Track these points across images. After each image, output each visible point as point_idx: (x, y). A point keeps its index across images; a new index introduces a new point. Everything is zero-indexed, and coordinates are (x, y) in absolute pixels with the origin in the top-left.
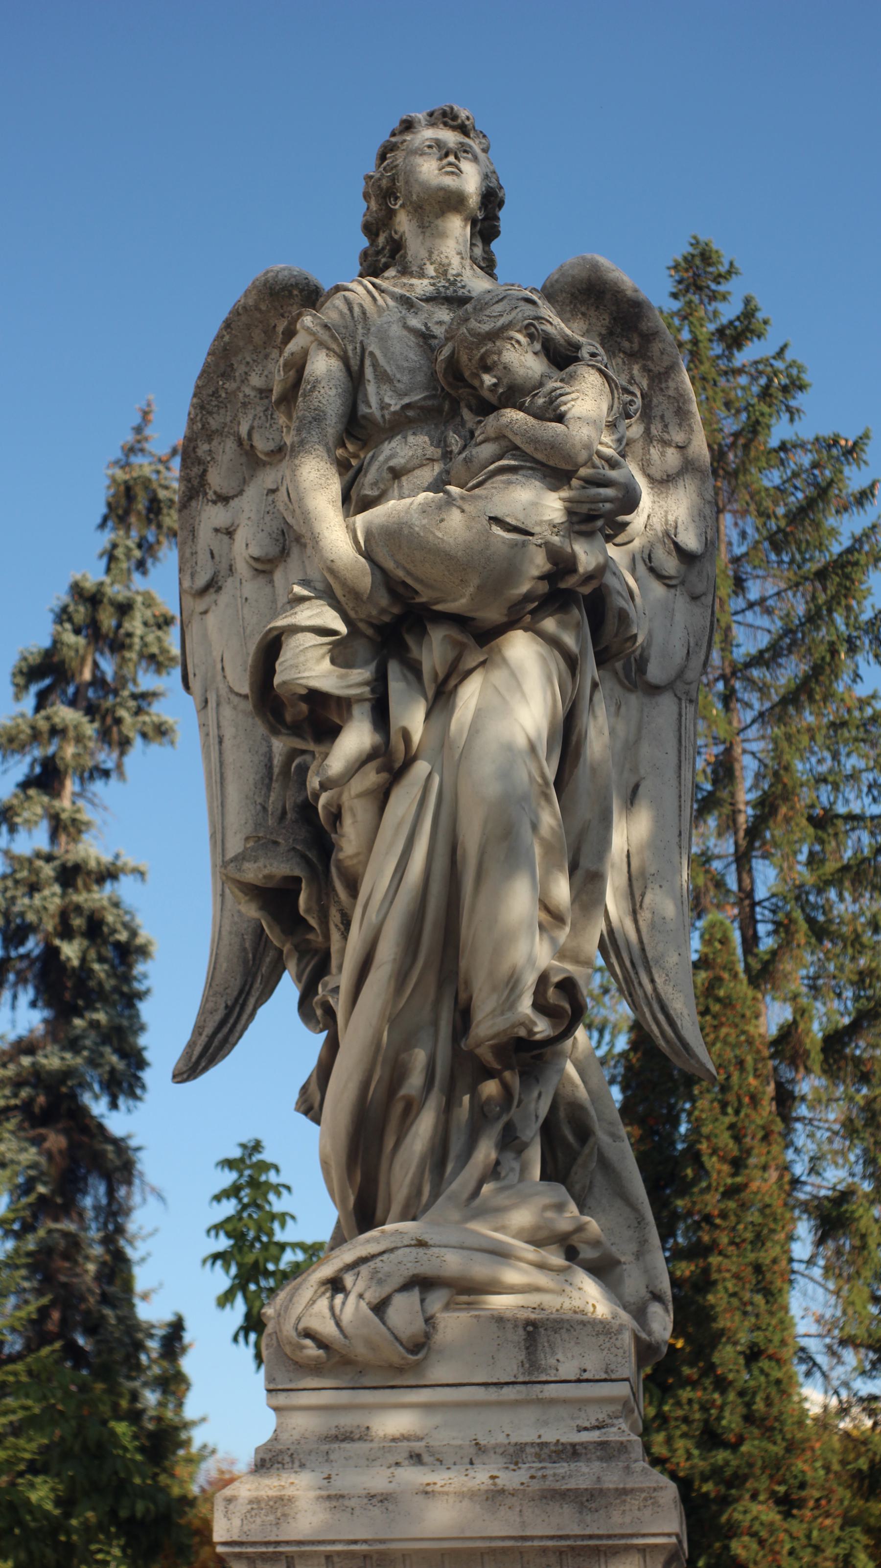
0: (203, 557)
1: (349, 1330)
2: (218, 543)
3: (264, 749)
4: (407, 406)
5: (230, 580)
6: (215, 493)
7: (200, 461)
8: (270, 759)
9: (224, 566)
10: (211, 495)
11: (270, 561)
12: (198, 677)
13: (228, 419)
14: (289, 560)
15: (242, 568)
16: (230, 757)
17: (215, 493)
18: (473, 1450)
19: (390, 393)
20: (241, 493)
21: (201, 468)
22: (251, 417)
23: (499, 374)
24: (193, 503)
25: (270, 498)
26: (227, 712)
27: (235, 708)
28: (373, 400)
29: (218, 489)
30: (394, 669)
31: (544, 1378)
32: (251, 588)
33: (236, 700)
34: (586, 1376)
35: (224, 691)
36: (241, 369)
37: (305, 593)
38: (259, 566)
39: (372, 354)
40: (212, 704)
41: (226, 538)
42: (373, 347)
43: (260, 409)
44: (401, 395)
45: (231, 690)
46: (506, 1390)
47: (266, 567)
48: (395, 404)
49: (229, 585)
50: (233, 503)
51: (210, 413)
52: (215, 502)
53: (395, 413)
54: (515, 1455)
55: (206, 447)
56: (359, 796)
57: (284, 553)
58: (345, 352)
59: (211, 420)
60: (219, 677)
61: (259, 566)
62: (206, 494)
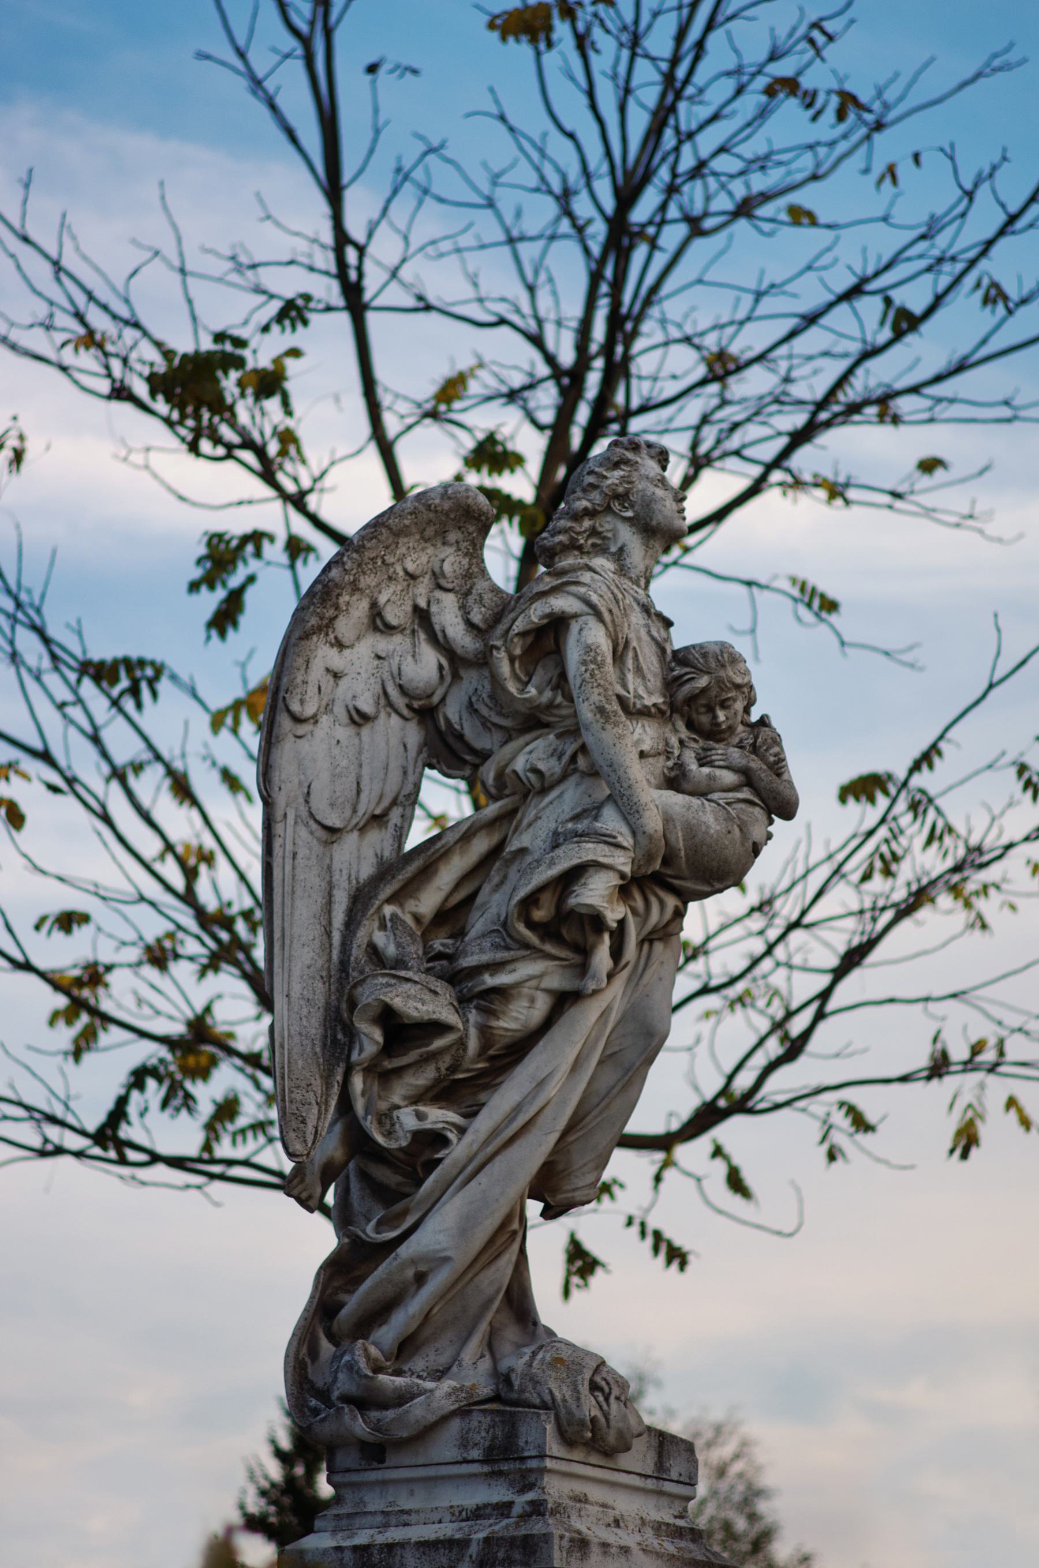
0: (312, 690)
1: (612, 1423)
2: (328, 682)
3: (328, 878)
4: (654, 705)
5: (325, 716)
6: (336, 638)
7: (337, 607)
8: (331, 886)
9: (324, 703)
10: (332, 636)
12: (283, 792)
13: (374, 584)
14: (376, 722)
15: (339, 711)
17: (336, 638)
18: (639, 1522)
20: (352, 646)
21: (336, 613)
22: (391, 591)
23: (729, 715)
24: (315, 638)
25: (376, 662)
26: (303, 832)
27: (312, 833)
28: (631, 687)
29: (340, 636)
31: (665, 1476)
32: (344, 733)
33: (314, 826)
34: (682, 1479)
35: (304, 813)
36: (402, 550)
38: (356, 717)
39: (634, 648)
41: (332, 680)
42: (634, 644)
43: (400, 588)
44: (650, 693)
45: (311, 815)
46: (649, 1481)
48: (649, 701)
49: (325, 720)
50: (347, 652)
51: (364, 573)
52: (332, 645)
53: (646, 707)
54: (659, 1528)
55: (347, 598)
56: (548, 991)
58: (617, 639)
59: (362, 578)
60: (301, 800)
61: (356, 717)
62: (327, 635)
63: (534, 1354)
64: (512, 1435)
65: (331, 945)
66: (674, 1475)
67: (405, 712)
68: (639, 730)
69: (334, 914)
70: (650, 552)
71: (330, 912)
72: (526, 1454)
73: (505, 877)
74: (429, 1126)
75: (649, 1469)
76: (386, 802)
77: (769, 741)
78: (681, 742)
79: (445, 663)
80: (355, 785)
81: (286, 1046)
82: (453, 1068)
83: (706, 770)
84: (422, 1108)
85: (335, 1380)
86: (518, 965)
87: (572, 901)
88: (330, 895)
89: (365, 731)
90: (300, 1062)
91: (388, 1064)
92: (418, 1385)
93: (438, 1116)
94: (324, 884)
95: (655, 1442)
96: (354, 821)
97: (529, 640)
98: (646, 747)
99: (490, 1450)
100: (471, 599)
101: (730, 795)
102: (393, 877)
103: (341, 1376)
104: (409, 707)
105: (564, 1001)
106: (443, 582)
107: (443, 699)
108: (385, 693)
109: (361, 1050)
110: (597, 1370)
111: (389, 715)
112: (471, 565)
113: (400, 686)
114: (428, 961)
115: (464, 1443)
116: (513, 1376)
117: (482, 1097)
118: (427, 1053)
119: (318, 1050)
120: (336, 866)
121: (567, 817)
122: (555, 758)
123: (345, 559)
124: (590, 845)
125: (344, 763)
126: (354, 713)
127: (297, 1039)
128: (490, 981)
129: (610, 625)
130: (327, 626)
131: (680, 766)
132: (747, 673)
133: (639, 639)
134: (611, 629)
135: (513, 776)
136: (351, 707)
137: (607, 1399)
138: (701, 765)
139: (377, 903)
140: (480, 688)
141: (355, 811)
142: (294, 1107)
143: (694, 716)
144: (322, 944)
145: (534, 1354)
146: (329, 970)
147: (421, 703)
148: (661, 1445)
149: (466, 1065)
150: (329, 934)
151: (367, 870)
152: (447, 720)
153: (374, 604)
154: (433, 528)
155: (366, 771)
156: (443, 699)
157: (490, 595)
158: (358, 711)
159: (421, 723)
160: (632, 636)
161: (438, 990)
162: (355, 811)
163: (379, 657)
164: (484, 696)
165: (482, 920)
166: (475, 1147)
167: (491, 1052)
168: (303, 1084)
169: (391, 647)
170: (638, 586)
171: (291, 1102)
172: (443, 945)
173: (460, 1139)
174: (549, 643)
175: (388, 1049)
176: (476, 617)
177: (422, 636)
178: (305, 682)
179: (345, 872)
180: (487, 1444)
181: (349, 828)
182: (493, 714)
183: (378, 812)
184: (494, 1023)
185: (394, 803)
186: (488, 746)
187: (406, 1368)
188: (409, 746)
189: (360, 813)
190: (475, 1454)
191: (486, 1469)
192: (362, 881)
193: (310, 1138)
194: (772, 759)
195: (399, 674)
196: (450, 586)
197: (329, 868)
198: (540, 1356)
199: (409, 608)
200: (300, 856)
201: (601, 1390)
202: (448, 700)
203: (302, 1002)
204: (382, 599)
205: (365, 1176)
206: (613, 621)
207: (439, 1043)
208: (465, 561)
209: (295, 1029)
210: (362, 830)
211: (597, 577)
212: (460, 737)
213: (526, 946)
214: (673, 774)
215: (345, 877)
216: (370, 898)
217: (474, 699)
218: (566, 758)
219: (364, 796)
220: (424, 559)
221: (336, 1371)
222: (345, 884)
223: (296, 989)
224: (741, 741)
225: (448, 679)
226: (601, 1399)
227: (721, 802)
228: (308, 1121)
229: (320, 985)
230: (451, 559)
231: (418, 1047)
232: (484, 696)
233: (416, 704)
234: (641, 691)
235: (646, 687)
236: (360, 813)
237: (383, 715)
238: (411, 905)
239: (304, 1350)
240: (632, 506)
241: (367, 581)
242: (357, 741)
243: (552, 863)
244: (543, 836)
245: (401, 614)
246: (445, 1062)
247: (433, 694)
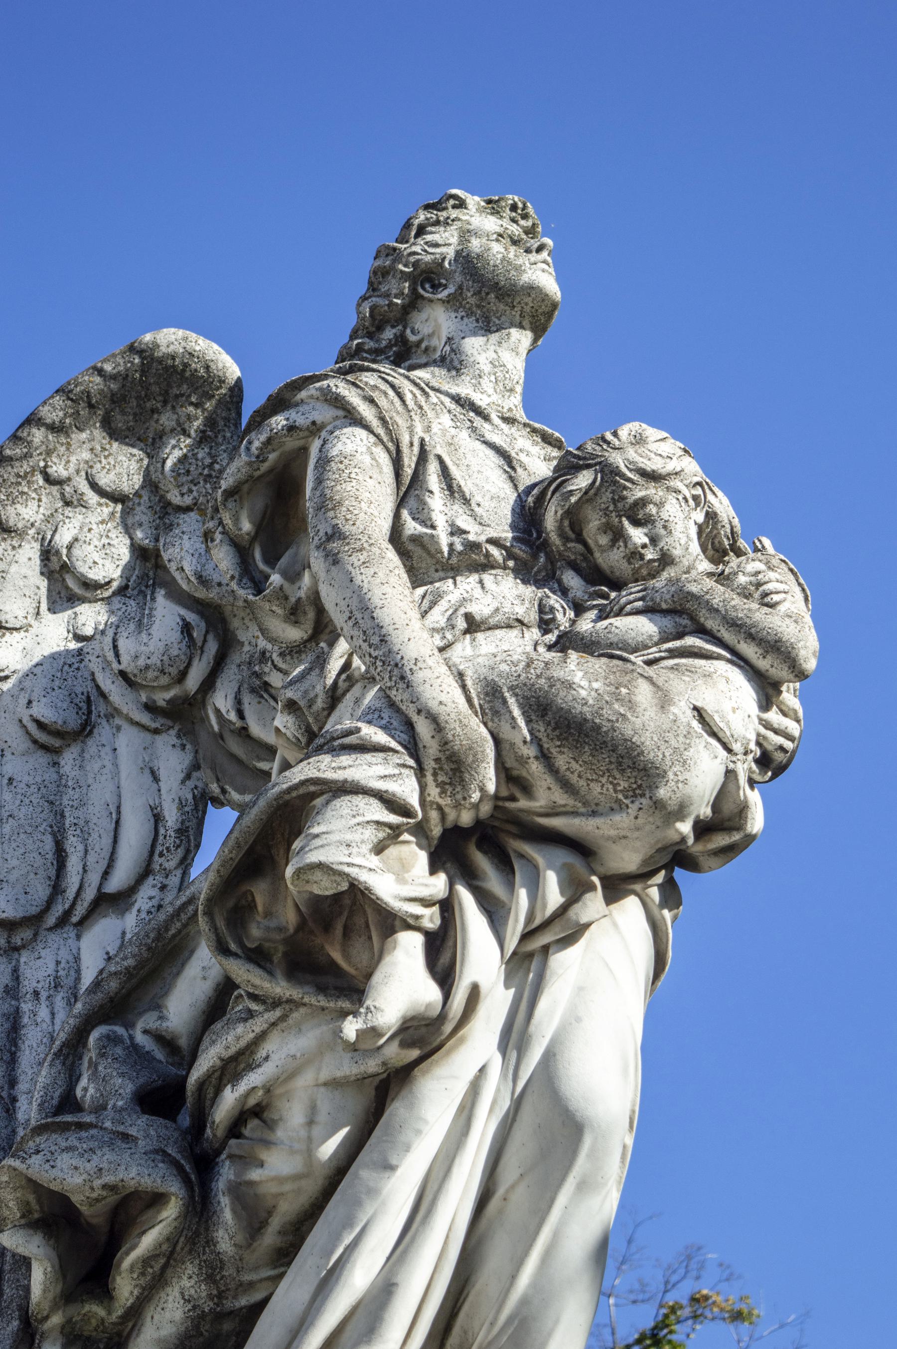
11: (58, 734)
19: (465, 517)
30: (466, 897)
37: (380, 737)
47: (56, 743)
57: (84, 731)
67: (144, 718)
79: (191, 617)
80: (49, 844)
86: (268, 1046)
89: (68, 759)
96: (58, 910)
97: (260, 502)
104: (150, 708)
106: (174, 497)
107: (209, 684)
108: (103, 695)
111: (119, 728)
113: (123, 674)
118: (146, 1261)
126: (32, 728)
129: (375, 423)
134: (381, 431)
136: (26, 721)
141: (57, 889)
147: (169, 695)
152: (218, 711)
153: (47, 553)
158: (40, 725)
161: (133, 1131)
162: (57, 889)
177: (160, 594)
184: (255, 1175)
188: (163, 774)
195: (117, 655)
196: (188, 500)
204: (63, 538)
206: (382, 419)
210: (82, 923)
212: (244, 733)
213: (276, 1003)
219: (74, 864)
233: (162, 698)
234: (464, 522)
235: (474, 516)
236: (71, 893)
237: (103, 731)
238: (148, 1021)
241: (29, 512)
242: (50, 775)
247: (182, 676)
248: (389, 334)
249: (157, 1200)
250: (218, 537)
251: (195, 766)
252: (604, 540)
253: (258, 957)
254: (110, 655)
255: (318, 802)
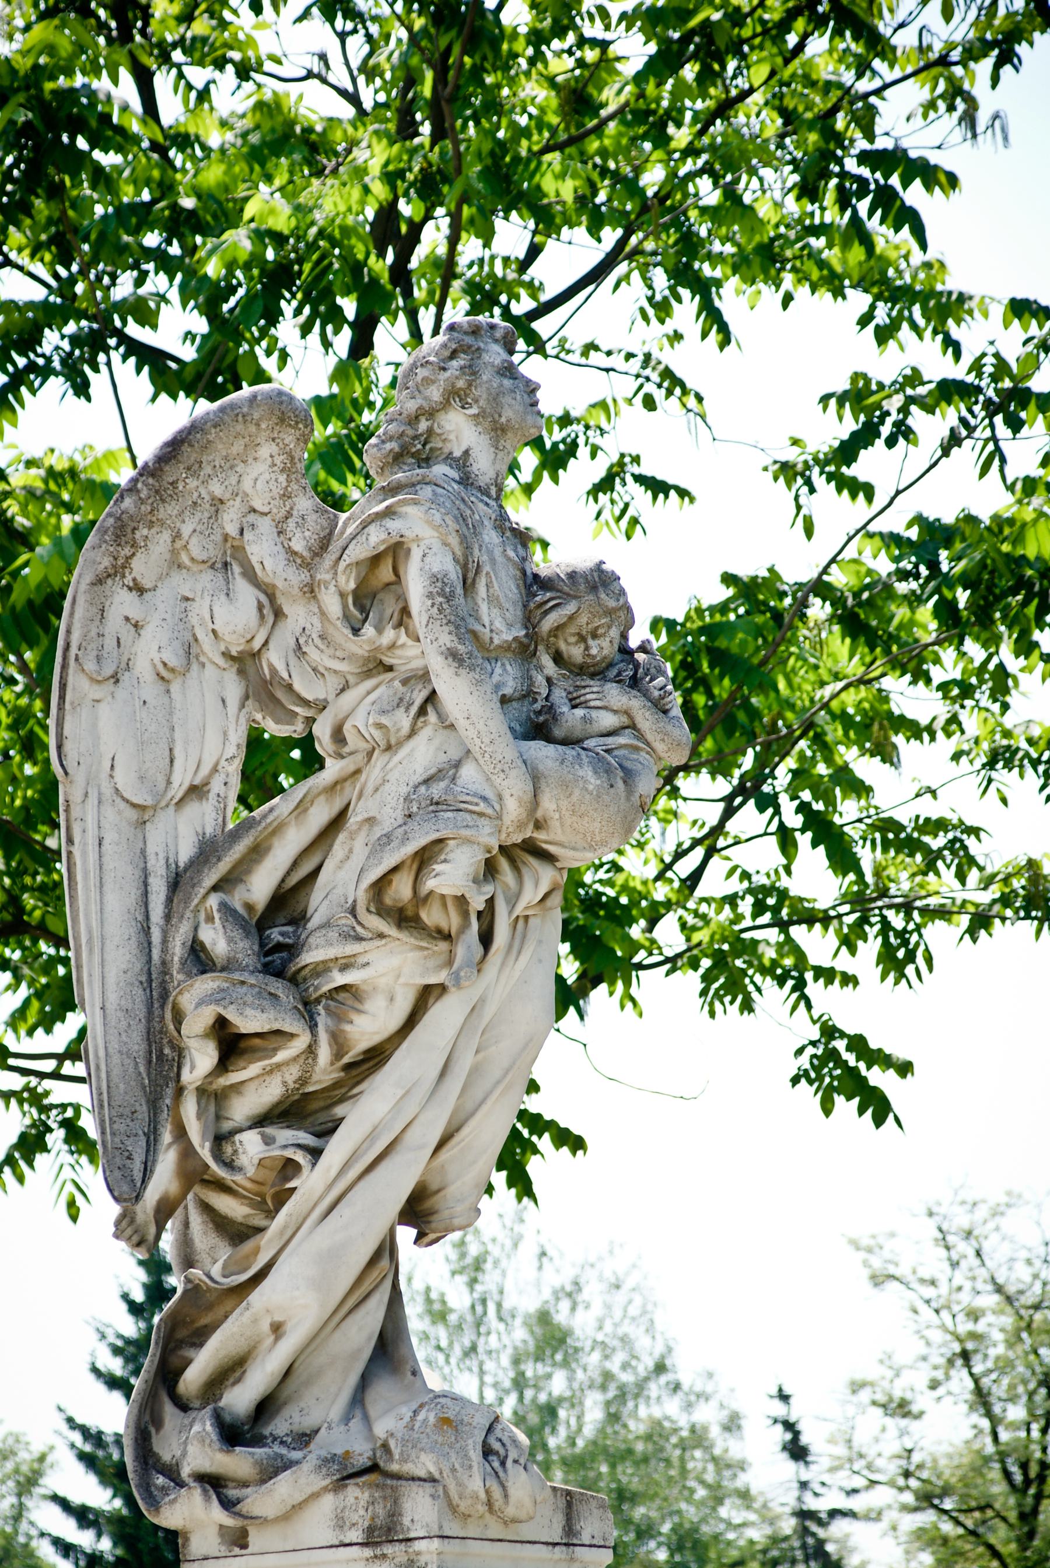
0: (110, 643)
2: (127, 633)
7: (134, 545)
9: (125, 659)
11: (172, 670)
16: (109, 863)
24: (109, 581)
26: (110, 814)
27: (119, 812)
28: (486, 620)
32: (150, 690)
33: (123, 805)
35: (108, 791)
36: (208, 469)
40: (93, 799)
42: (487, 568)
43: (206, 515)
50: (147, 596)
51: (163, 501)
52: (130, 589)
55: (145, 532)
56: (406, 985)
62: (123, 576)
63: (415, 1413)
64: (394, 1515)
65: (150, 943)
66: (586, 1539)
67: (221, 661)
68: (498, 670)
69: (151, 906)
70: (501, 455)
71: (146, 904)
72: (412, 1535)
73: (351, 851)
74: (277, 1153)
75: (556, 1534)
76: (205, 771)
77: (653, 671)
78: (549, 680)
79: (263, 598)
81: (103, 1067)
82: (303, 1081)
83: (579, 712)
84: (269, 1130)
85: (184, 1454)
87: (430, 884)
88: (146, 884)
90: (122, 1086)
91: (224, 1081)
92: (282, 1456)
93: (288, 1138)
94: (138, 873)
95: (562, 1503)
98: (508, 691)
99: (370, 1530)
100: (291, 523)
101: (610, 740)
102: (219, 859)
103: (191, 1449)
105: (426, 996)
109: (193, 1068)
110: (490, 1429)
112: (289, 481)
113: (214, 631)
114: (266, 955)
115: (340, 1523)
116: (392, 1443)
117: (339, 1111)
119: (142, 1069)
120: (151, 849)
121: (420, 779)
122: (402, 709)
123: (140, 485)
124: (450, 814)
125: (152, 728)
127: (116, 1059)
128: (340, 979)
130: (124, 567)
131: (550, 709)
132: (622, 592)
133: (493, 561)
135: (354, 731)
137: (503, 1464)
138: (574, 707)
139: (202, 891)
140: (308, 626)
141: (169, 782)
142: (117, 1140)
143: (563, 646)
144: (140, 944)
145: (415, 1413)
146: (150, 974)
148: (569, 1505)
149: (315, 1077)
150: (146, 931)
151: (185, 852)
154: (242, 442)
155: (178, 735)
156: (266, 643)
157: (315, 516)
158: (165, 664)
159: (241, 672)
160: (485, 558)
163: (187, 599)
164: (315, 636)
165: (326, 902)
166: (334, 1173)
167: (346, 1059)
168: (127, 1111)
169: (199, 587)
170: (489, 496)
171: (113, 1134)
172: (282, 934)
173: (314, 1165)
174: (385, 573)
175: (224, 1064)
176: (298, 545)
177: (236, 569)
178: (100, 635)
179: (162, 856)
180: (366, 1524)
181: (163, 804)
182: (325, 658)
183: (196, 782)
185: (215, 770)
186: (322, 697)
187: (266, 1432)
189: (176, 784)
190: (355, 1535)
191: (368, 1552)
192: (181, 864)
193: (138, 1176)
194: (656, 693)
196: (266, 509)
197: (143, 852)
198: (421, 1417)
199: (218, 538)
200: (105, 842)
201: (497, 1453)
202: (271, 645)
203: (119, 1014)
204: (186, 530)
205: (207, 1208)
207: (281, 1056)
208: (282, 478)
209: (114, 1046)
211: (440, 490)
212: (289, 687)
213: (381, 936)
214: (541, 719)
215: (162, 862)
216: (193, 886)
217: (302, 641)
218: (414, 709)
220: (233, 480)
221: (185, 1443)
222: (162, 871)
223: (113, 998)
224: (619, 674)
225: (270, 619)
226: (496, 1464)
227: (599, 750)
228: (135, 1156)
229: (140, 992)
230: (267, 476)
231: (260, 1060)
232: (315, 636)
234: (499, 624)
239: (147, 1418)
240: (476, 401)
242: (166, 700)
243: (405, 839)
244: (393, 803)
245: (211, 547)
246: (292, 1074)
248: (423, 425)
249: (292, 1036)
250: (332, 589)
251: (247, 697)
252: (573, 640)
253: (382, 911)
254: (208, 617)
255: (451, 843)
